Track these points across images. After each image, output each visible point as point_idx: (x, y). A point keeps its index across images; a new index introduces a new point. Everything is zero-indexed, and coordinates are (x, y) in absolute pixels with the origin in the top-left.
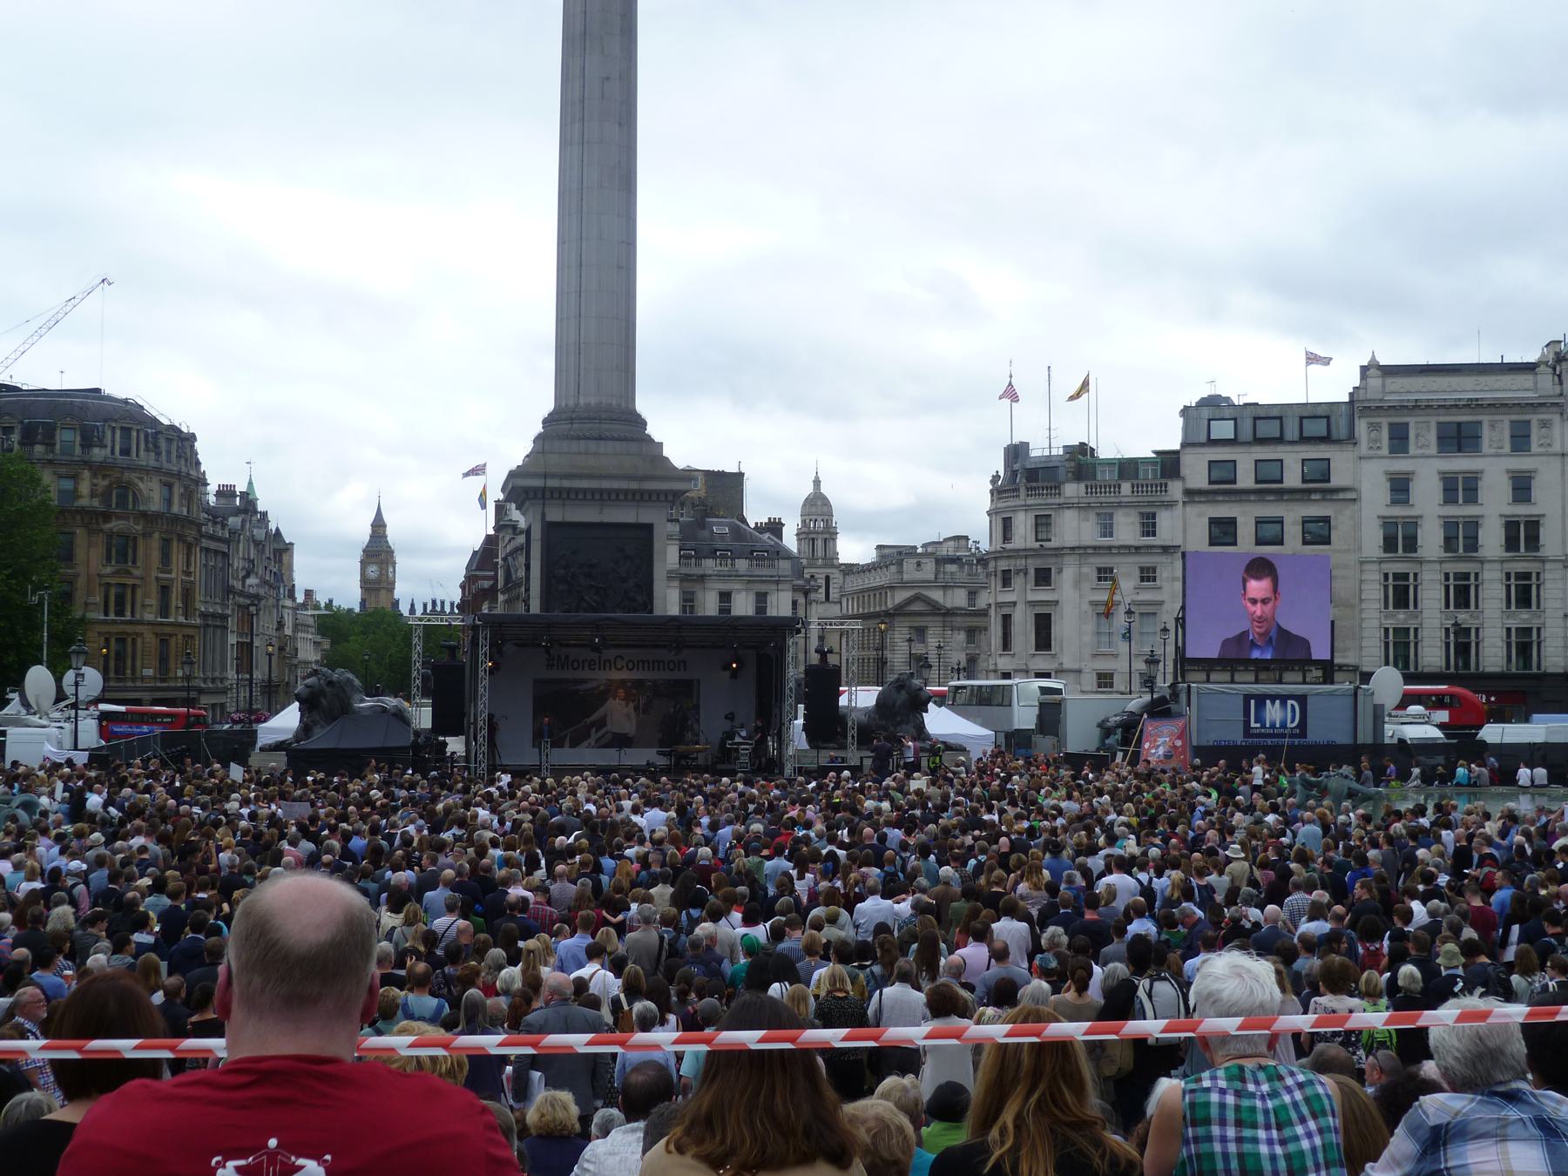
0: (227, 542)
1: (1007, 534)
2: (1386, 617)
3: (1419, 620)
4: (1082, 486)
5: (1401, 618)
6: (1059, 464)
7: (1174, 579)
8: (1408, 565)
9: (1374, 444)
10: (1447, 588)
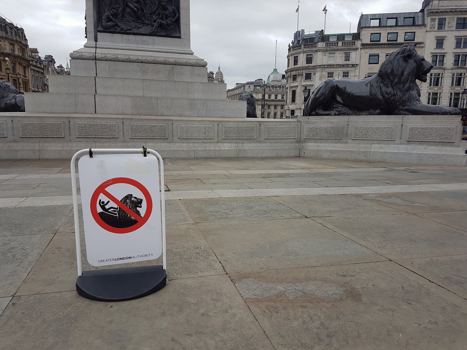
0: (43, 69)
1: (296, 62)
2: (430, 89)
3: (442, 89)
4: (325, 43)
5: (436, 89)
6: (315, 37)
7: (355, 76)
8: (440, 70)
9: (432, 27)
10: (453, 79)
